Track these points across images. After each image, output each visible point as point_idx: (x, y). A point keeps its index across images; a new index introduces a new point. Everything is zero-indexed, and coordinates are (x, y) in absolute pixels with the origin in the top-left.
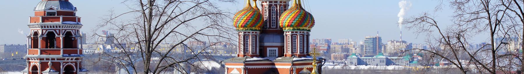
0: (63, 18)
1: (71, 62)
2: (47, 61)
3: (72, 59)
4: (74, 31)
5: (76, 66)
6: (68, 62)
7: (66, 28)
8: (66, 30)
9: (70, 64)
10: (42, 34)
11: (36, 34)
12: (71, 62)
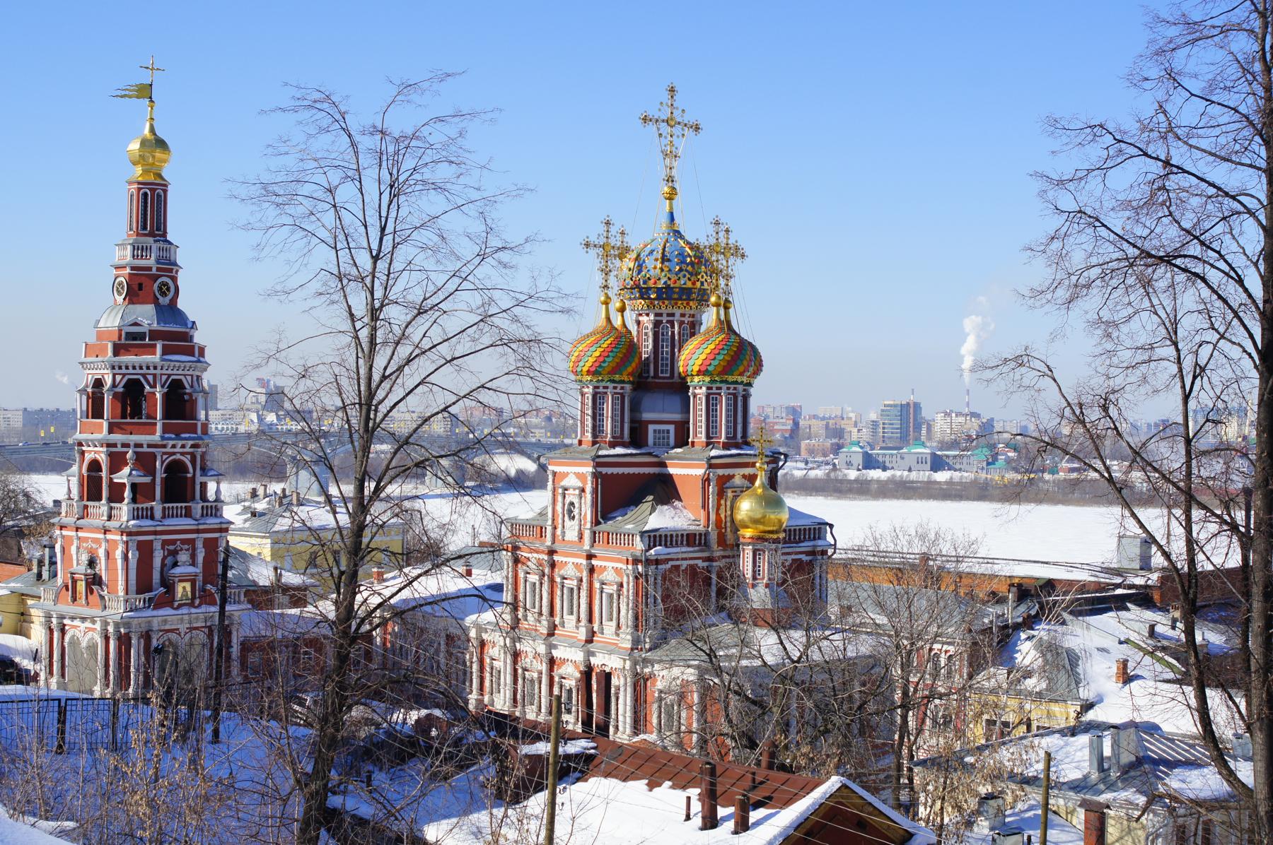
0: (164, 346)
1: (182, 454)
2: (125, 450)
3: (183, 446)
4: (189, 378)
5: (193, 461)
6: (174, 454)
7: (169, 372)
8: (169, 376)
9: (178, 457)
10: (114, 385)
11: (98, 383)
12: (182, 454)
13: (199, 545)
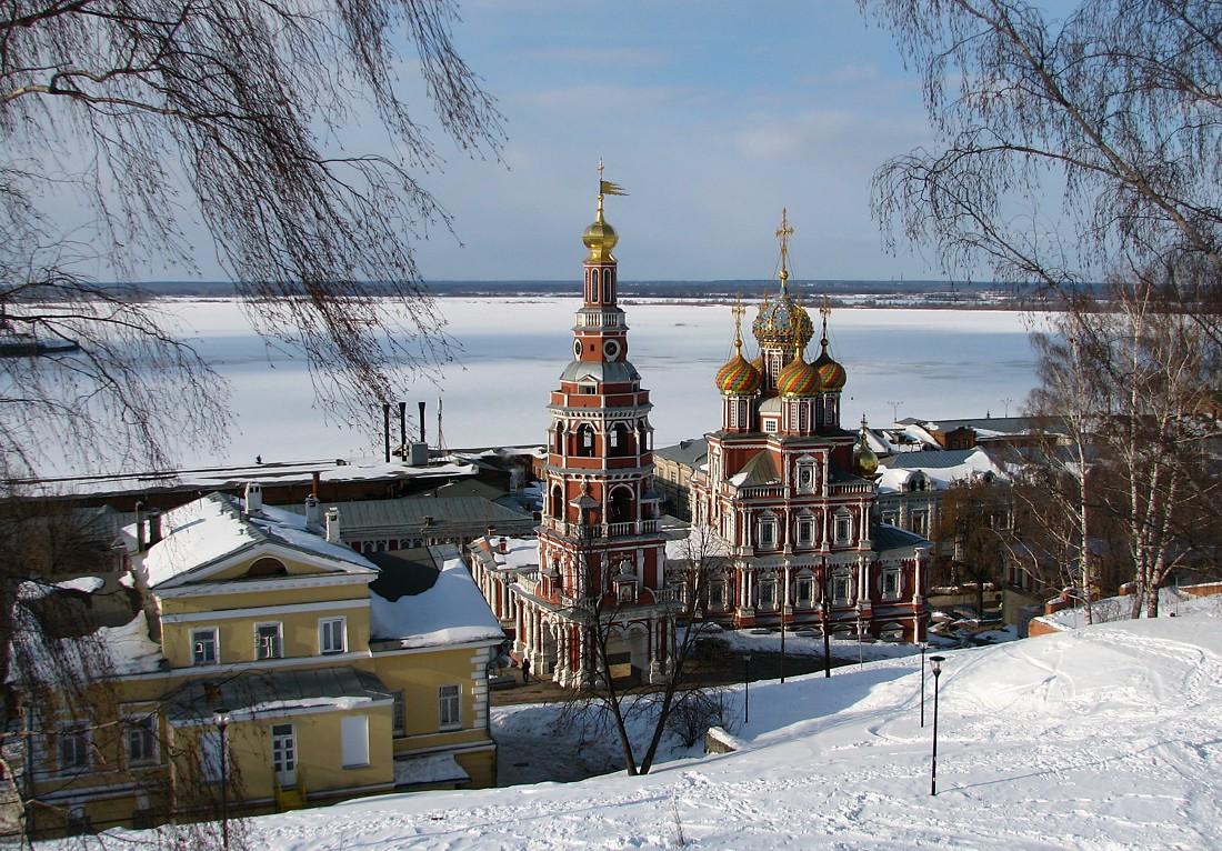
0: (606, 399)
1: (624, 482)
3: (626, 477)
5: (635, 488)
6: (618, 483)
11: (560, 425)
12: (624, 482)
13: (640, 553)
